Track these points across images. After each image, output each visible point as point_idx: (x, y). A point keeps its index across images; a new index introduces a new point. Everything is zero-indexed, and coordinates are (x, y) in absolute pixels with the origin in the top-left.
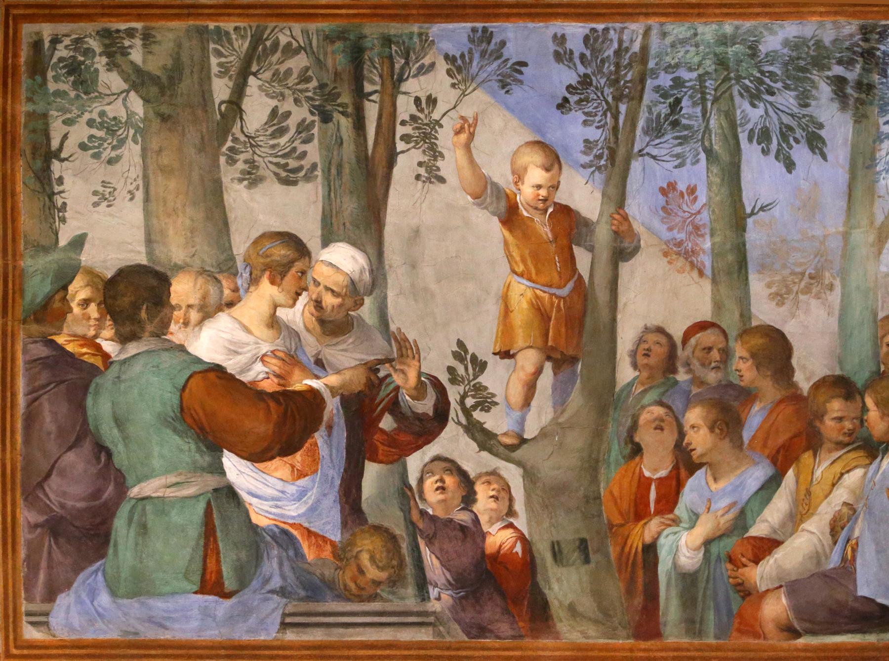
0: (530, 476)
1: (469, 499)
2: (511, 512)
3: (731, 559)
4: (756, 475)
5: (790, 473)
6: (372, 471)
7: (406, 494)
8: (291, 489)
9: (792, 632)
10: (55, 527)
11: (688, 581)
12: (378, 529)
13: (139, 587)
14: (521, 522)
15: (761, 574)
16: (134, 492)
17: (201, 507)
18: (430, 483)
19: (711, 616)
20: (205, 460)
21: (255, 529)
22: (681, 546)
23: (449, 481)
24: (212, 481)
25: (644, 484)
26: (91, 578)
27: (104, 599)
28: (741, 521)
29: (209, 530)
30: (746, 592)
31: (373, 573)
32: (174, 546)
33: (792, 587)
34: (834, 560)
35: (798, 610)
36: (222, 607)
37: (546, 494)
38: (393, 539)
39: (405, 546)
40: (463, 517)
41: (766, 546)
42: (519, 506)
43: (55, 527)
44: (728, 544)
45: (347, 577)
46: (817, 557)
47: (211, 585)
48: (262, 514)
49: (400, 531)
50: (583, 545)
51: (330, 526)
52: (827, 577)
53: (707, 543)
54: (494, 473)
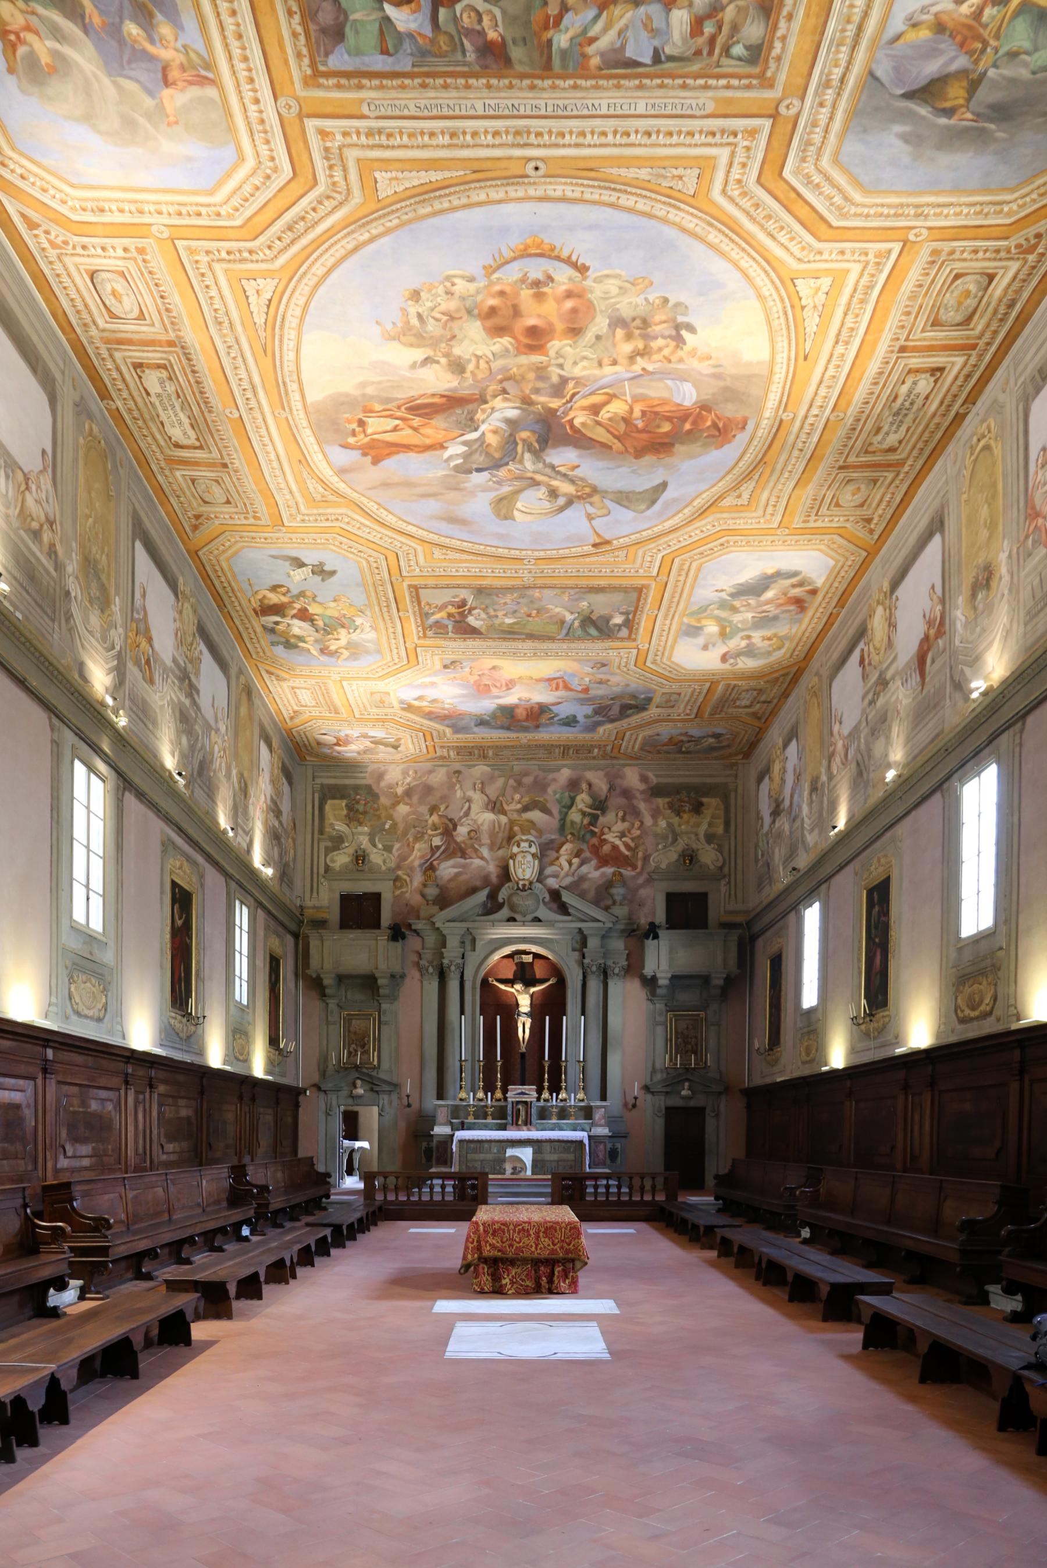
0: (504, 12)
1: (480, 21)
2: (496, 25)
3: (580, 45)
4: (592, 13)
5: (605, 13)
6: (442, 12)
7: (455, 20)
8: (412, 18)
9: (601, 69)
10: (324, 31)
11: (564, 54)
12: (446, 33)
13: (358, 52)
14: (501, 29)
15: (590, 50)
16: (352, 17)
17: (377, 25)
18: (465, 16)
19: (571, 64)
20: (377, 6)
21: (399, 33)
22: (562, 40)
23: (473, 14)
24: (380, 14)
25: (548, 17)
26: (340, 49)
27: (346, 57)
28: (585, 31)
29: (382, 33)
30: (585, 56)
31: (445, 48)
32: (370, 37)
33: (602, 54)
34: (618, 44)
35: (603, 61)
36: (390, 60)
37: (510, 19)
38: (451, 36)
39: (457, 39)
40: (478, 27)
41: (593, 40)
42: (500, 23)
43: (324, 31)
44: (578, 40)
45: (435, 49)
46: (612, 43)
47: (385, 51)
48: (401, 27)
49: (454, 33)
50: (524, 39)
51: (428, 31)
52: (615, 51)
53: (571, 39)
54: (490, 12)
